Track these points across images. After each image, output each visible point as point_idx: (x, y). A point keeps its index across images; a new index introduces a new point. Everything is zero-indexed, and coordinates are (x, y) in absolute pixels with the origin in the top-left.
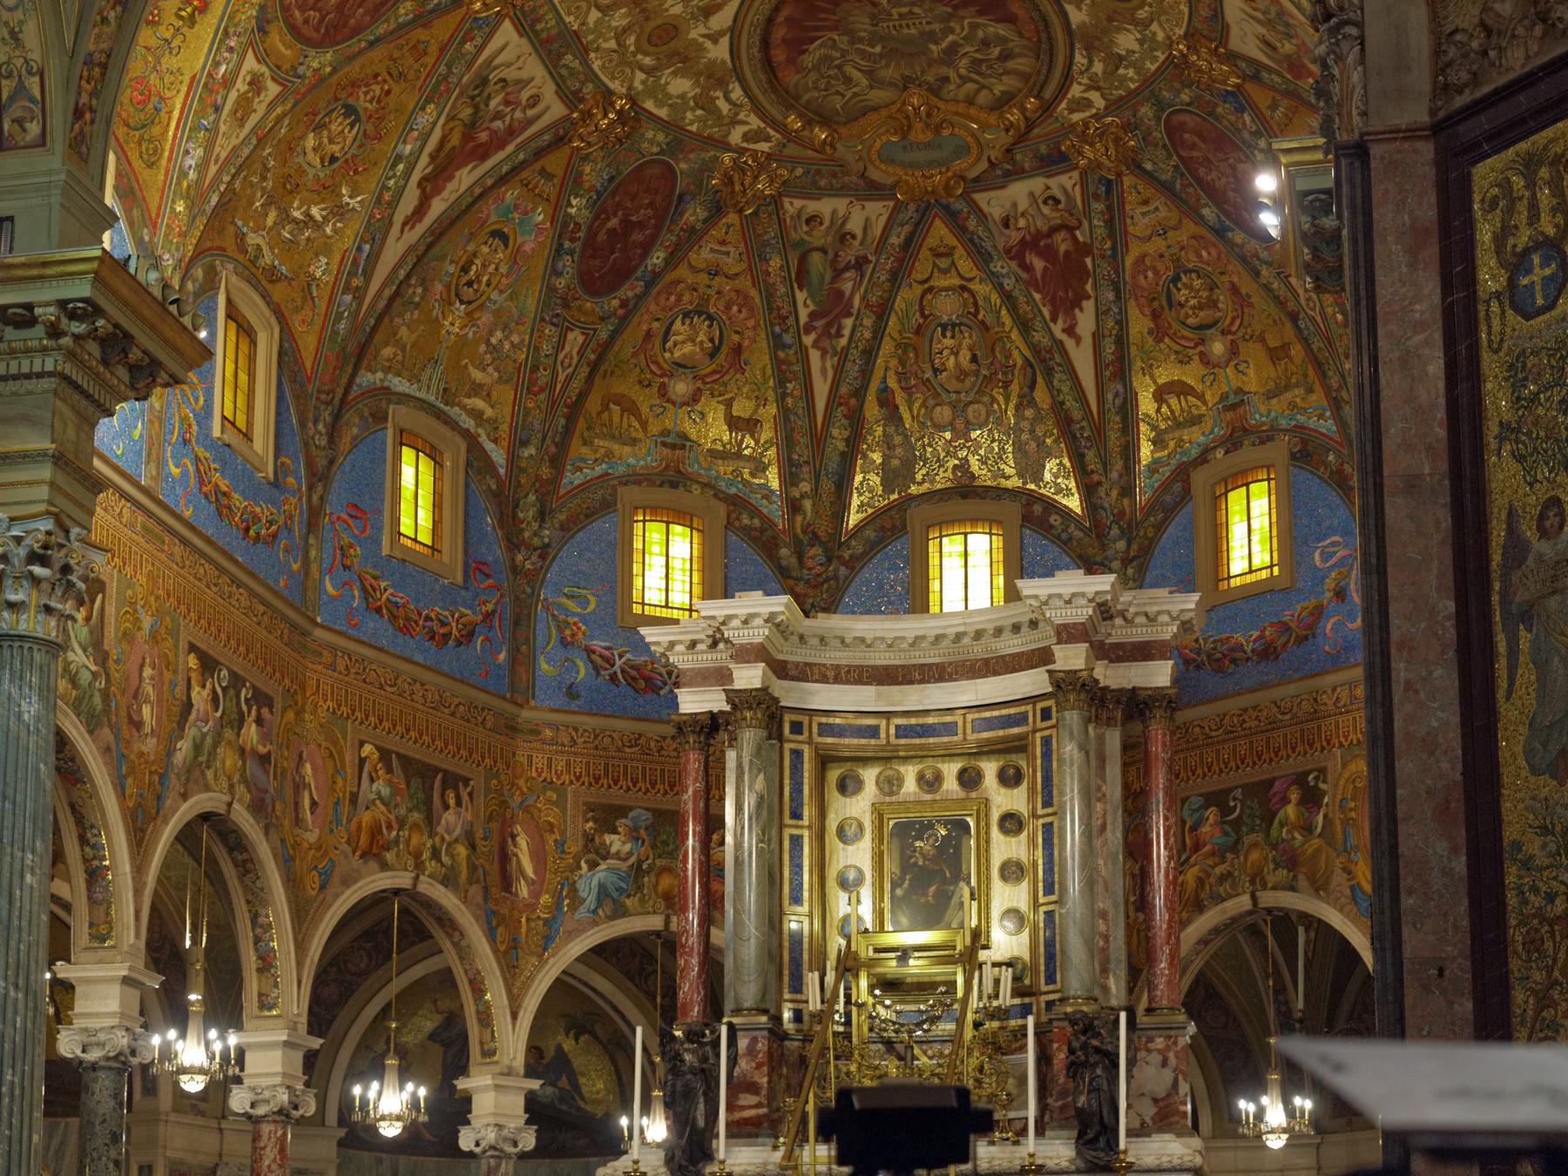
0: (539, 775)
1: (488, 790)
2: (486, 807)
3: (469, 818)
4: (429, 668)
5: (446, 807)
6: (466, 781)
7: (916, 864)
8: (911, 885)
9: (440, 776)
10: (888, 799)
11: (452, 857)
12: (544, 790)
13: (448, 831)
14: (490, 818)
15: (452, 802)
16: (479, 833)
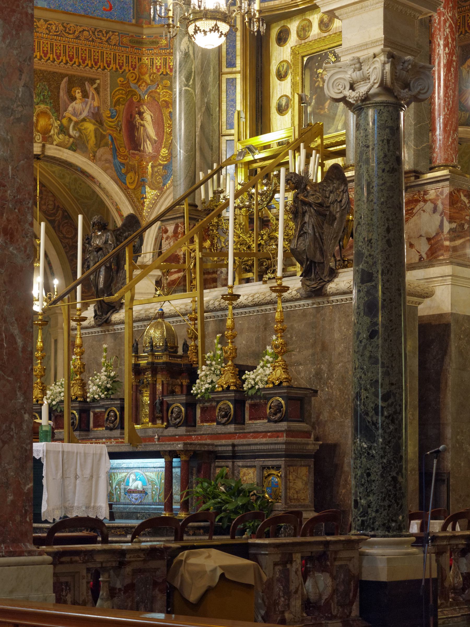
0: (158, 70)
1: (114, 85)
2: (112, 97)
3: (96, 104)
4: (54, 11)
5: (73, 99)
6: (92, 81)
7: (319, 85)
8: (316, 103)
9: (65, 80)
10: (303, 42)
11: (80, 131)
12: (162, 79)
13: (75, 114)
14: (118, 102)
15: (78, 95)
16: (106, 114)
